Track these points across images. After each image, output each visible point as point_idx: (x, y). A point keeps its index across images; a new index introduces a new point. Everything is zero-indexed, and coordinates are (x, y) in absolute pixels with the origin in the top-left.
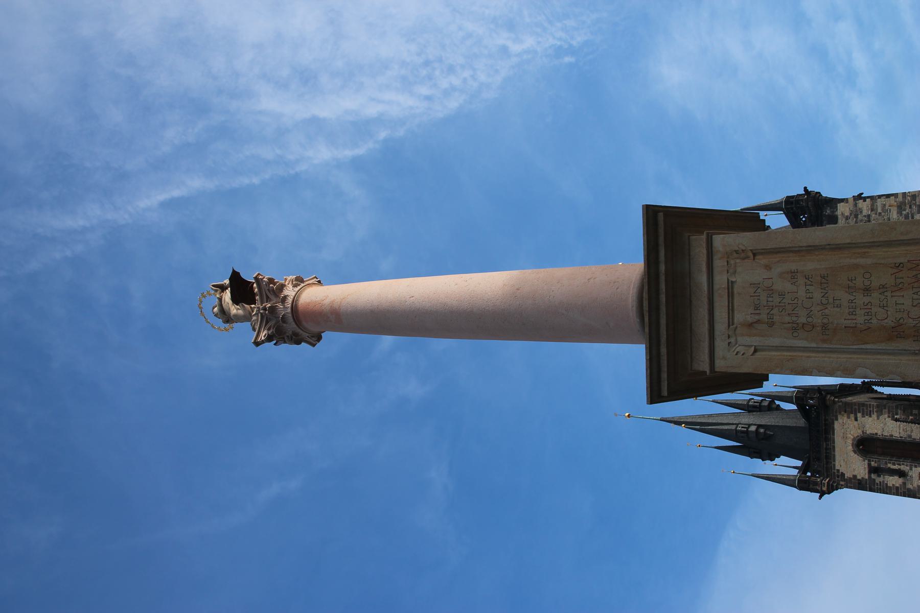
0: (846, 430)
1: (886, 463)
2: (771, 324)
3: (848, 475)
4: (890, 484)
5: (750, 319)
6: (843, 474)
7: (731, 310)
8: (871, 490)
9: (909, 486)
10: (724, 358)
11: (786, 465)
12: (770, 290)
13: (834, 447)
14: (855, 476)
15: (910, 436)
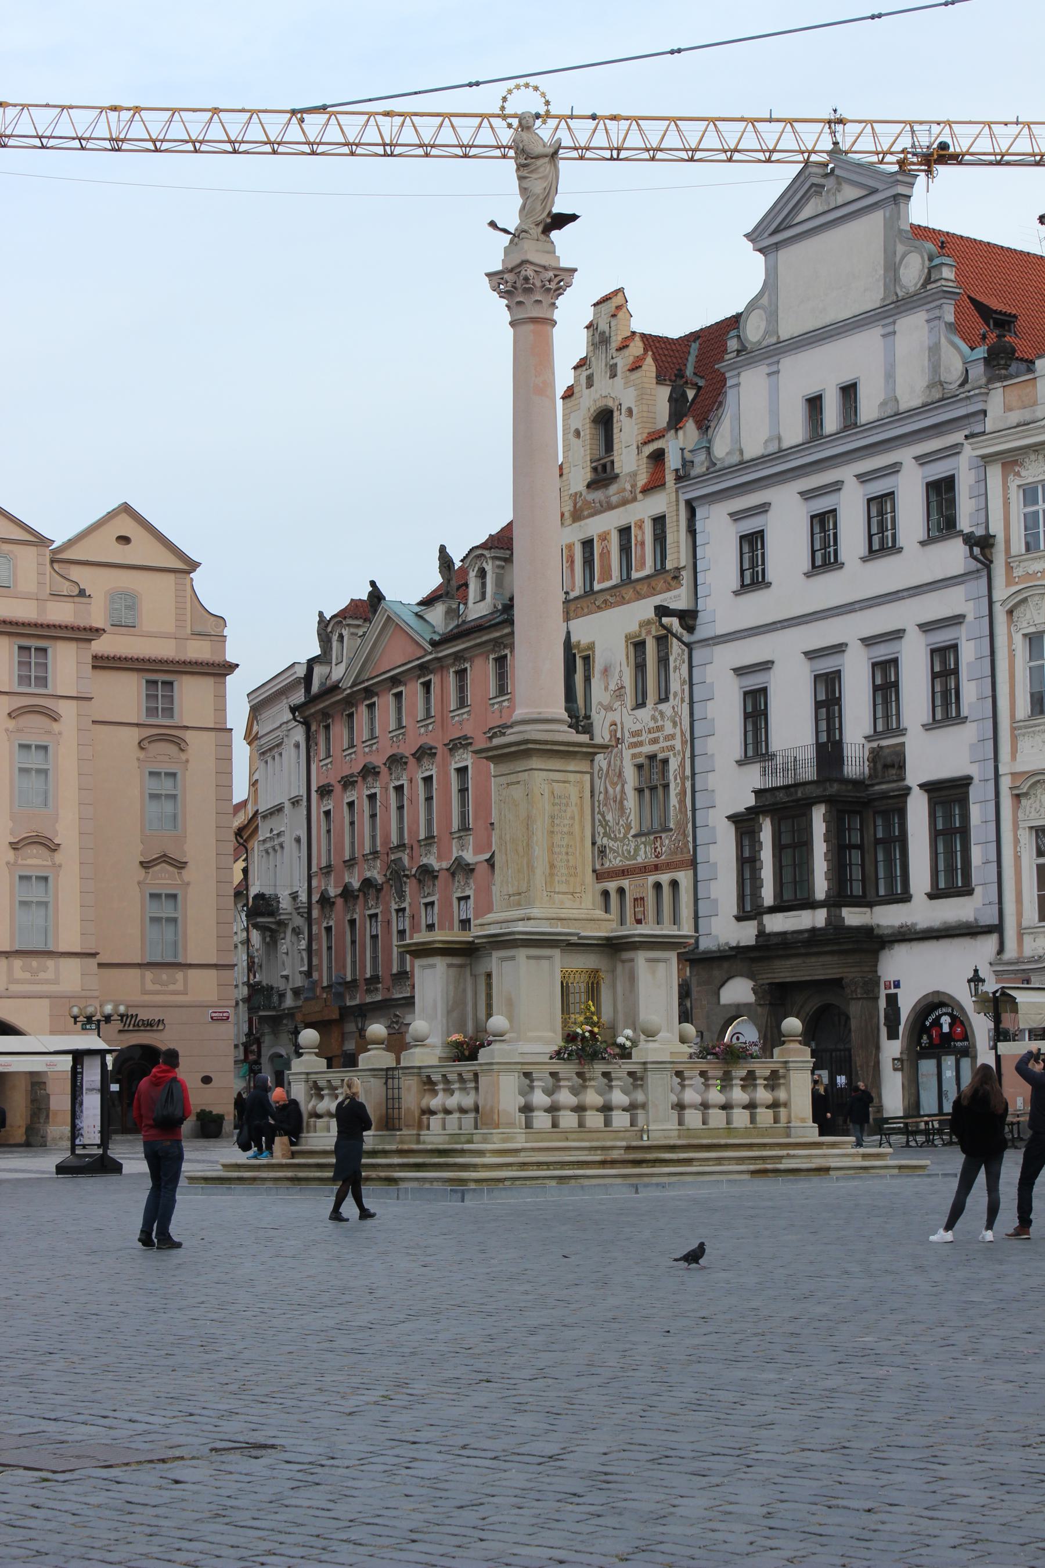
2: (554, 805)
7: (558, 781)
12: (567, 805)
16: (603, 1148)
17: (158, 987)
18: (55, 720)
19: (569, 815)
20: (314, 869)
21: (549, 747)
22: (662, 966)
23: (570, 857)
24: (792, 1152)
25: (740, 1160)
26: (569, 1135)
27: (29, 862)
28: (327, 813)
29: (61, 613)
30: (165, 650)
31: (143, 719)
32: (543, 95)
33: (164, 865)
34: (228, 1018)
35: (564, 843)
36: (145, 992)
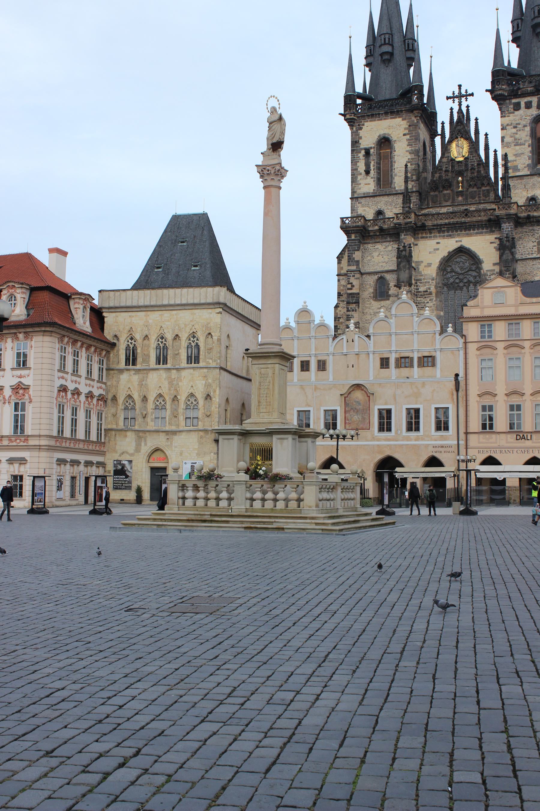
0: (396, 127)
1: (374, 160)
3: (361, 133)
4: (358, 164)
6: (361, 129)
7: (264, 368)
8: (352, 151)
9: (359, 177)
11: (362, 79)
13: (381, 120)
14: (361, 138)
15: (396, 175)
16: (200, 515)
21: (254, 355)
22: (285, 441)
24: (277, 520)
25: (242, 522)
26: (199, 509)
32: (276, 98)
35: (265, 393)
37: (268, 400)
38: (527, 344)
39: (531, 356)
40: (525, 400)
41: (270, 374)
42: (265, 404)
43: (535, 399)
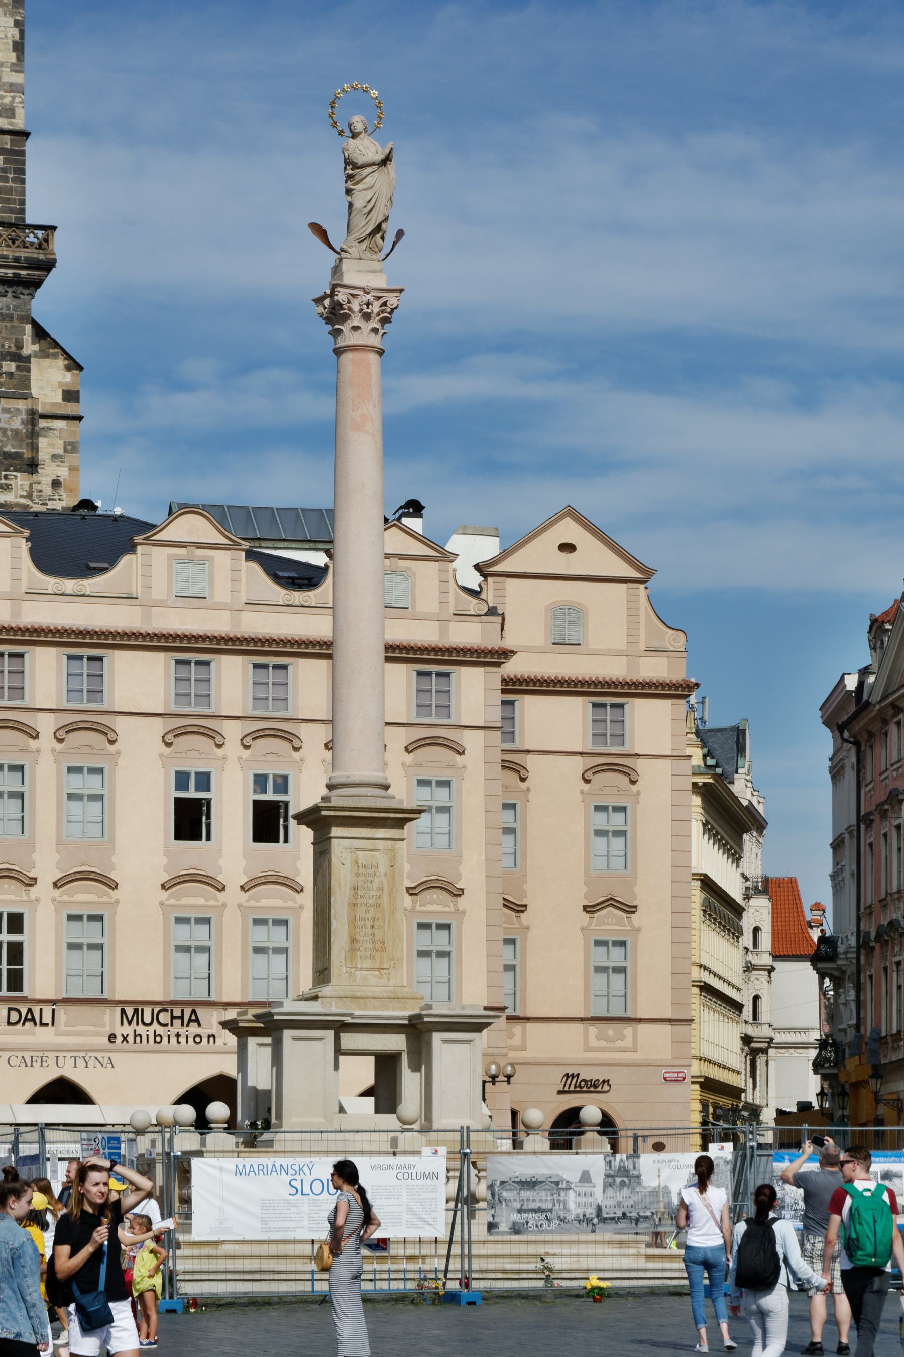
2: (357, 875)
5: (360, 862)
7: (364, 850)
10: (339, 845)
17: (603, 1044)
18: (460, 754)
19: (376, 884)
20: (862, 910)
23: (376, 931)
27: (429, 908)
28: (871, 845)
29: (468, 634)
30: (614, 669)
31: (589, 748)
33: (610, 909)
34: (684, 1078)
35: (370, 916)
36: (588, 1049)
37: (377, 938)
38: (46, 724)
39: (55, 761)
40: (38, 900)
41: (383, 868)
42: (371, 946)
43: (66, 898)
